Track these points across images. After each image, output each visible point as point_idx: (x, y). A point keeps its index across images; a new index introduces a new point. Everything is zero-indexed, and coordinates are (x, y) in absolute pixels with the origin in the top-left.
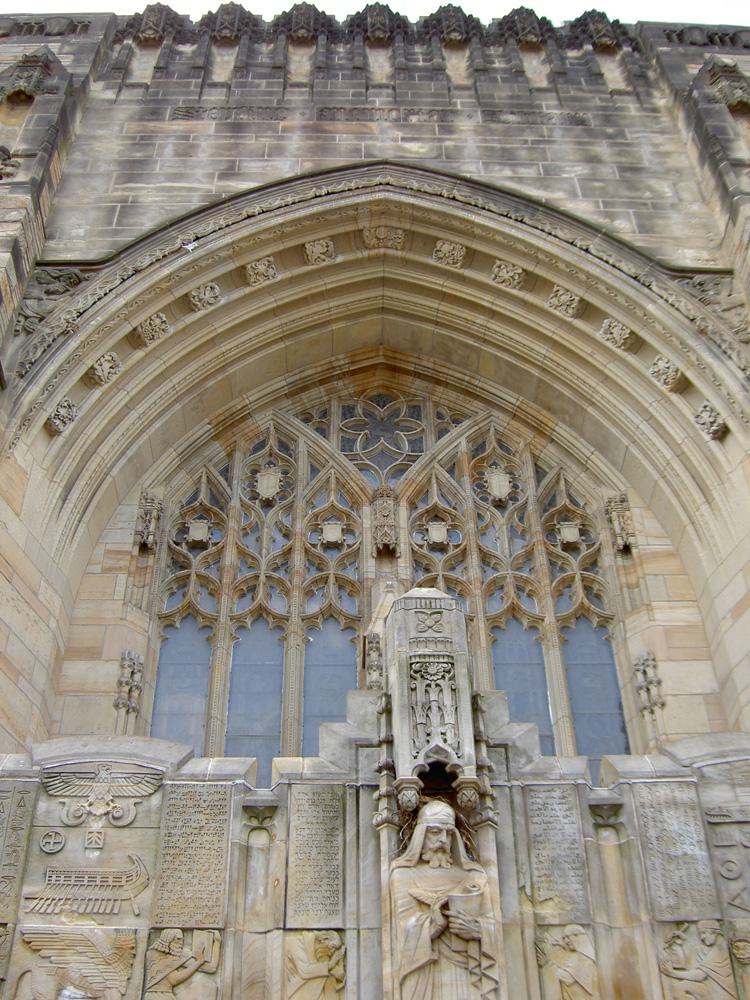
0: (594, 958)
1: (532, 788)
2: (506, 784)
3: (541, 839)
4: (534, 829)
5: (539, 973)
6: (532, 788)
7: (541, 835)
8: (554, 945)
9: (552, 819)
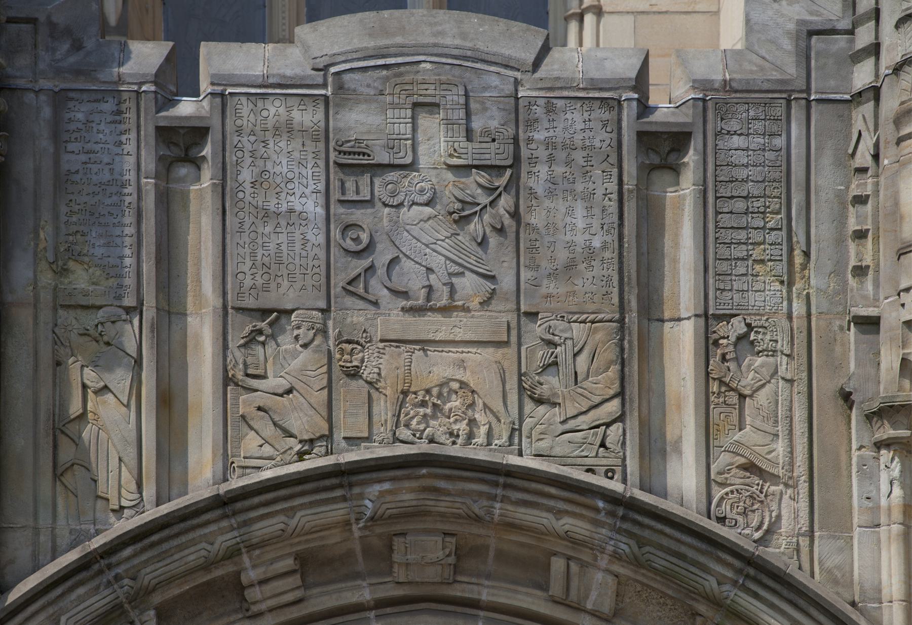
0: (135, 355)
1: (71, 95)
2: (29, 86)
3: (77, 178)
4: (72, 161)
5: (55, 375)
6: (71, 95)
7: (77, 172)
8: (81, 335)
9: (97, 147)
